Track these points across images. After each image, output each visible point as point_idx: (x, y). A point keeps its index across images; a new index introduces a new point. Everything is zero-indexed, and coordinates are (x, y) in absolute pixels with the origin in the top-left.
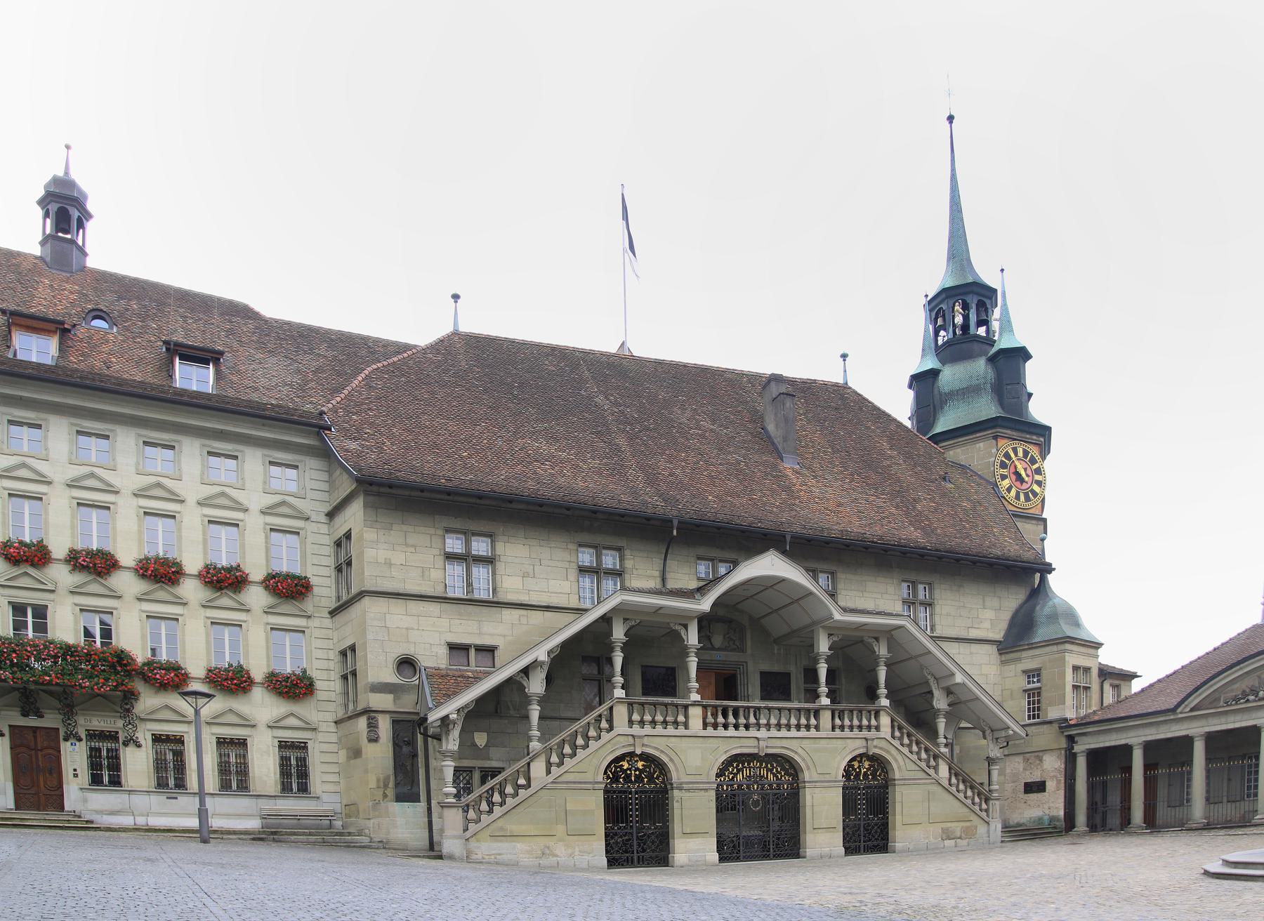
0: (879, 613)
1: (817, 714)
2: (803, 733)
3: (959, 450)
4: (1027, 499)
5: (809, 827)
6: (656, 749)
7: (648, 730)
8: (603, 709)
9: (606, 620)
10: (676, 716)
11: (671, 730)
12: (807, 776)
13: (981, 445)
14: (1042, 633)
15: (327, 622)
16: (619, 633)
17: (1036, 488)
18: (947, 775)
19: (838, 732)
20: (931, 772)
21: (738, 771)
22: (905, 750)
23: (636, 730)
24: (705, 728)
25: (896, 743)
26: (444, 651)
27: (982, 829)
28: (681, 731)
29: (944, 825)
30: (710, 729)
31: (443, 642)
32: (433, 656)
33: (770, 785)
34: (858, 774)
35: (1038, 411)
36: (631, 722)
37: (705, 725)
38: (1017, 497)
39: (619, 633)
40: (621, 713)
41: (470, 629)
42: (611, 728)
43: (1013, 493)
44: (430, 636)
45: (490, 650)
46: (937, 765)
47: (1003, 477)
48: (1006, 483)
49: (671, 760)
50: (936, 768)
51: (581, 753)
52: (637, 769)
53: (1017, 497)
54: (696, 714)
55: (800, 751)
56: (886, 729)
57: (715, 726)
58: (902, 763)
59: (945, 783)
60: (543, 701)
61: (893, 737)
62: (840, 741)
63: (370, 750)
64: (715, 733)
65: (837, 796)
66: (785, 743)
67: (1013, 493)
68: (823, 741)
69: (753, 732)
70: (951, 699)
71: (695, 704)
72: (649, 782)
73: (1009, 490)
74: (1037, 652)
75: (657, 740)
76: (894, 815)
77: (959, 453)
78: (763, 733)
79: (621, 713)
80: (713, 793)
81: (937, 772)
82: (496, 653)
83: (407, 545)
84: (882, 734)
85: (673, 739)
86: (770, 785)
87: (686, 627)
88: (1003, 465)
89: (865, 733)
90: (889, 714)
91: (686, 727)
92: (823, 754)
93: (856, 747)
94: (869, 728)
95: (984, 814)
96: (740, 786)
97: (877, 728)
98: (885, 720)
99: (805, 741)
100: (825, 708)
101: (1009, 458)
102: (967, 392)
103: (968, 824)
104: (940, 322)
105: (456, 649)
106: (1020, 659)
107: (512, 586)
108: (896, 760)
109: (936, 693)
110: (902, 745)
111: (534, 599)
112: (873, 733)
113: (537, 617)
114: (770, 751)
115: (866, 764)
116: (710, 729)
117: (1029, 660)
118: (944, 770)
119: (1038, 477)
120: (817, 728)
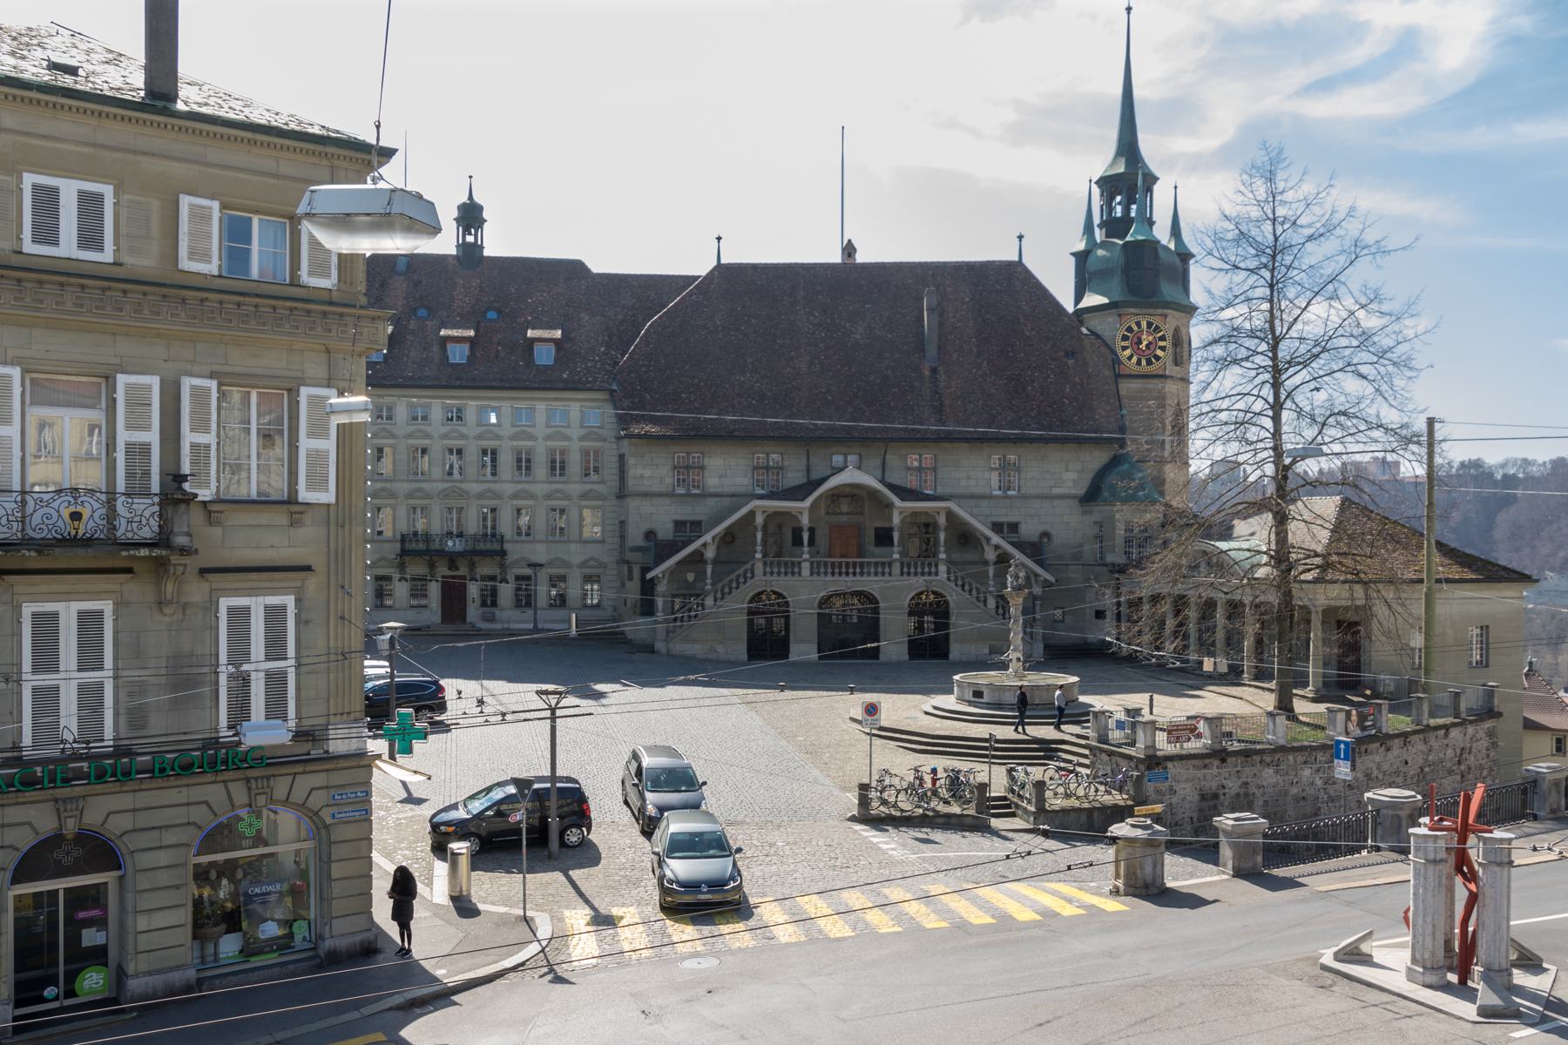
1: (890, 564)
4: (1149, 362)
7: (775, 577)
8: (748, 566)
9: (752, 514)
10: (792, 569)
11: (789, 577)
15: (615, 502)
16: (759, 520)
23: (768, 577)
26: (671, 526)
28: (796, 577)
32: (665, 531)
38: (1139, 363)
39: (759, 520)
41: (685, 512)
43: (1135, 359)
44: (662, 517)
45: (699, 523)
47: (1124, 348)
48: (1128, 352)
50: (985, 601)
51: (735, 592)
53: (1139, 363)
54: (806, 566)
56: (943, 575)
59: (993, 612)
60: (715, 562)
63: (629, 584)
67: (1135, 359)
69: (844, 578)
73: (1130, 358)
75: (781, 583)
78: (851, 577)
88: (1125, 338)
92: (894, 590)
94: (930, 574)
97: (937, 574)
98: (942, 568)
105: (679, 525)
106: (1091, 512)
107: (712, 482)
111: (726, 490)
113: (727, 501)
117: (1098, 512)
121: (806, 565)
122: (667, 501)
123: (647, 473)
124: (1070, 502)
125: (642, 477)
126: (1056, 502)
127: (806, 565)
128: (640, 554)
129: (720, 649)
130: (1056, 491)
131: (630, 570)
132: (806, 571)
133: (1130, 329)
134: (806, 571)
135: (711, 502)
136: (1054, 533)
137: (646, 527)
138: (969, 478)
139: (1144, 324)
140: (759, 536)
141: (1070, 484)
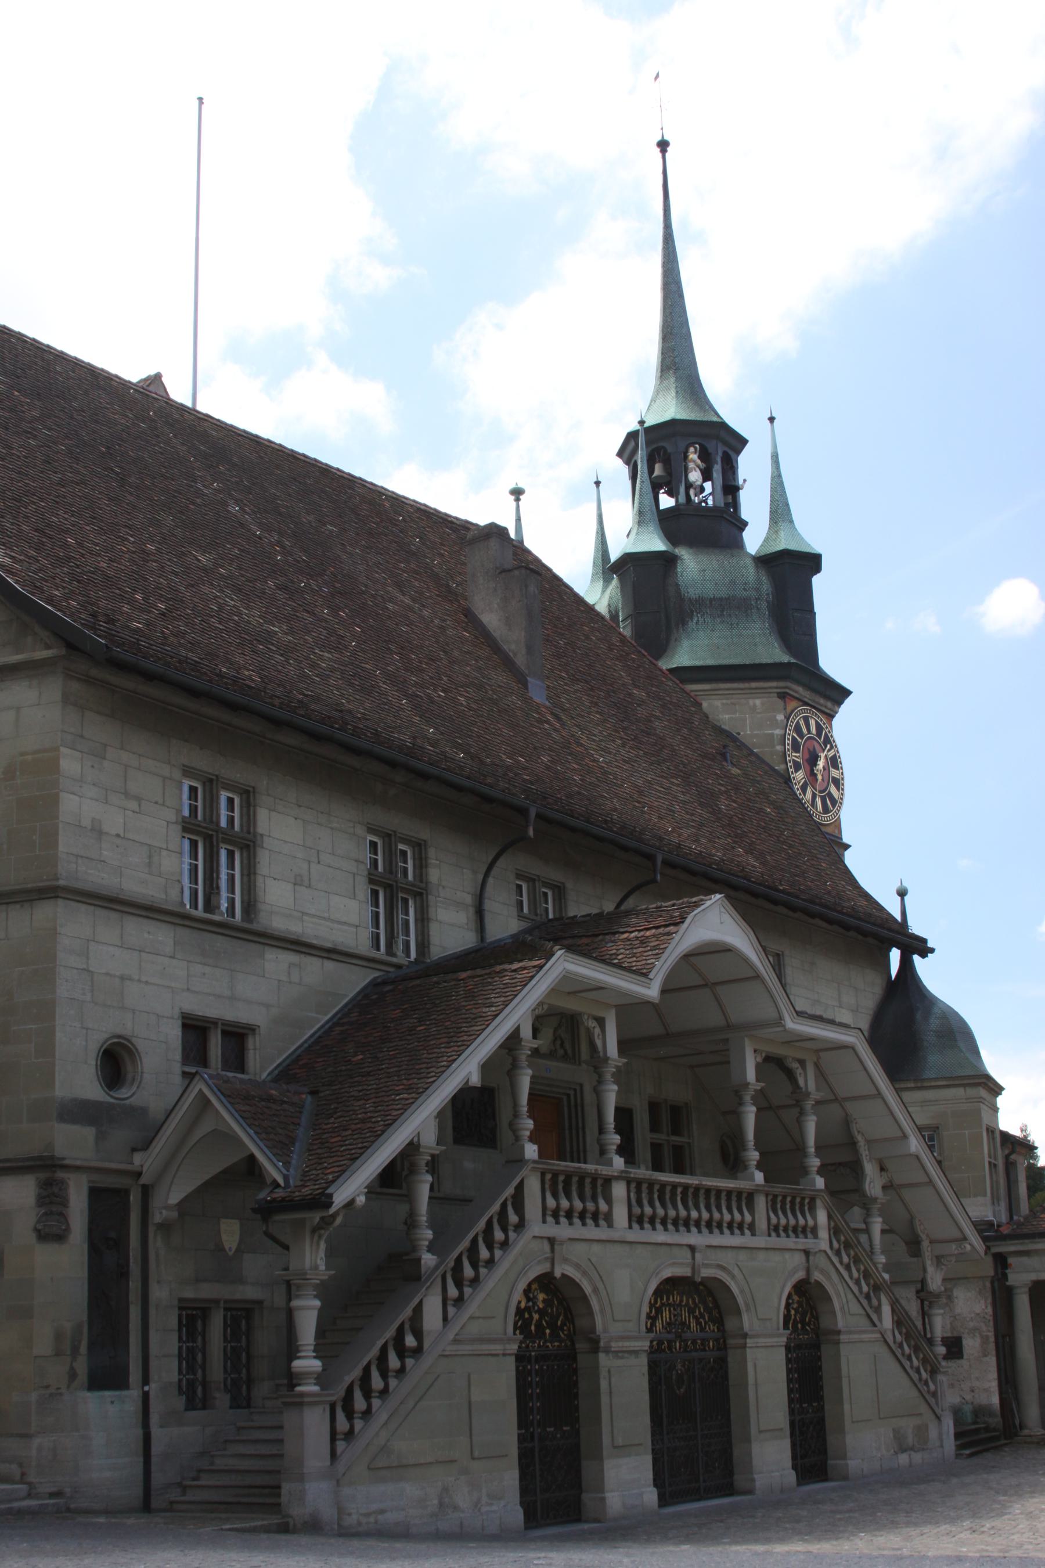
0: (819, 1019)
1: (750, 1197)
3: (718, 703)
4: (826, 810)
5: (754, 1431)
6: (577, 1266)
12: (748, 1322)
13: (758, 702)
14: (935, 1061)
17: (833, 789)
31: (176, 1013)
33: (694, 1342)
35: (832, 660)
42: (520, 1226)
43: (809, 795)
46: (880, 1305)
49: (596, 1290)
50: (878, 1310)
55: (736, 1272)
57: (640, 1221)
61: (831, 1247)
67: (809, 795)
68: (762, 1255)
72: (554, 1335)
73: (804, 789)
74: (930, 1095)
76: (840, 1401)
77: (723, 708)
80: (644, 1360)
82: (250, 1043)
83: (127, 794)
85: (596, 1248)
86: (694, 1342)
88: (796, 747)
91: (610, 1225)
97: (814, 1231)
101: (801, 736)
102: (728, 607)
104: (658, 470)
108: (838, 1295)
109: (870, 1169)
119: (834, 773)
120: (752, 1227)
122: (162, 935)
123: (114, 821)
125: (98, 831)
127: (619, 1190)
128: (89, 1132)
129: (463, 1498)
131: (51, 1198)
132: (620, 1214)
133: (798, 729)
135: (277, 962)
137: (104, 1027)
139: (813, 729)
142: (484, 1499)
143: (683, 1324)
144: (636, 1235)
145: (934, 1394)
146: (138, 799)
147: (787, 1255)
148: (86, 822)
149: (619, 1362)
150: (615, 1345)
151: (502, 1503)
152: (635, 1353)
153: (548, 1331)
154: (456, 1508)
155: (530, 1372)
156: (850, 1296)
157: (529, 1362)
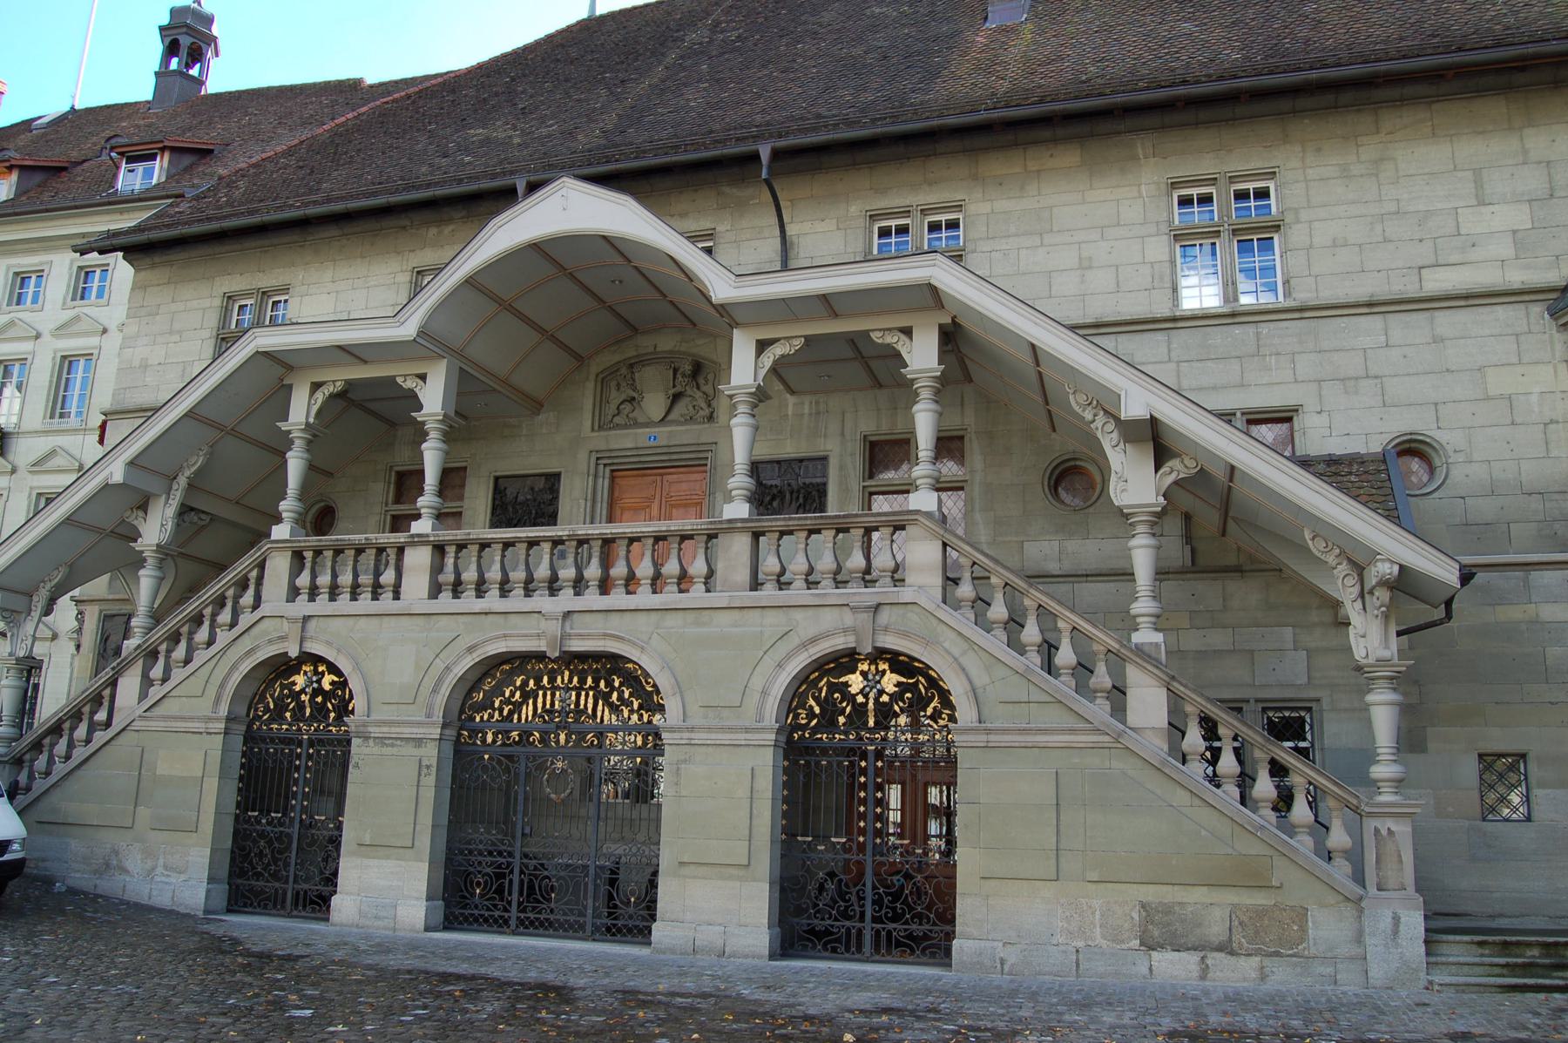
2: (670, 597)
6: (329, 643)
10: (377, 575)
18: (1160, 718)
19: (769, 593)
20: (1100, 709)
21: (526, 696)
22: (996, 643)
23: (302, 606)
24: (755, 585)
25: (963, 621)
27: (1327, 927)
28: (387, 603)
29: (1151, 894)
30: (446, 596)
34: (860, 710)
36: (294, 592)
37: (435, 590)
39: (301, 410)
40: (279, 566)
42: (256, 605)
52: (319, 691)
58: (981, 679)
59: (1157, 745)
62: (772, 617)
64: (375, 607)
65: (758, 769)
66: (615, 624)
70: (1176, 469)
71: (419, 540)
79: (279, 566)
81: (1119, 710)
84: (906, 594)
87: (423, 377)
89: (857, 593)
90: (935, 535)
91: (397, 596)
93: (827, 626)
95: (1340, 870)
96: (525, 734)
97: (897, 575)
99: (672, 620)
100: (732, 526)
103: (1260, 899)
110: (981, 622)
112: (883, 590)
114: (577, 646)
115: (890, 682)
116: (446, 596)
118: (1148, 703)
121: (418, 560)
124: (1503, 314)
126: (1447, 322)
130: (1439, 281)
132: (416, 581)
134: (416, 581)
136: (1446, 438)
138: (1085, 266)
140: (295, 465)
141: (1505, 249)
142: (160, 870)
143: (579, 712)
144: (446, 601)
145: (1355, 857)
146: (180, 332)
147: (798, 615)
148: (136, 363)
149: (376, 750)
150: (375, 731)
151: (183, 877)
152: (419, 742)
153: (332, 715)
154: (127, 871)
155: (299, 756)
156: (1001, 672)
157: (300, 744)
